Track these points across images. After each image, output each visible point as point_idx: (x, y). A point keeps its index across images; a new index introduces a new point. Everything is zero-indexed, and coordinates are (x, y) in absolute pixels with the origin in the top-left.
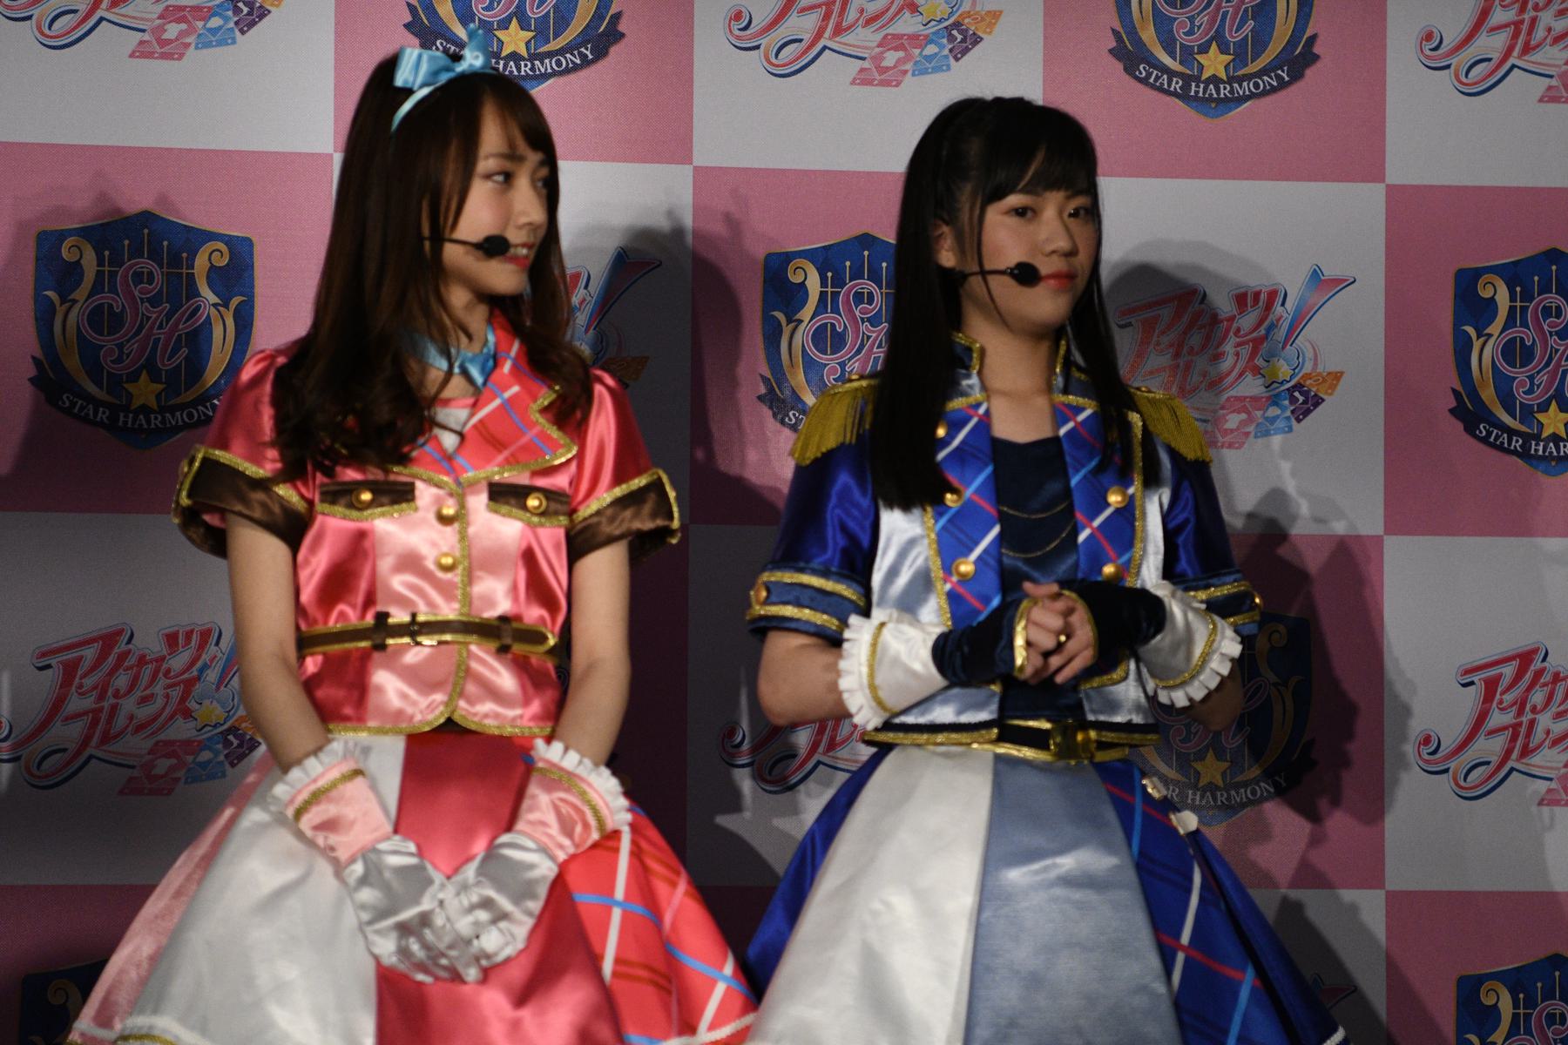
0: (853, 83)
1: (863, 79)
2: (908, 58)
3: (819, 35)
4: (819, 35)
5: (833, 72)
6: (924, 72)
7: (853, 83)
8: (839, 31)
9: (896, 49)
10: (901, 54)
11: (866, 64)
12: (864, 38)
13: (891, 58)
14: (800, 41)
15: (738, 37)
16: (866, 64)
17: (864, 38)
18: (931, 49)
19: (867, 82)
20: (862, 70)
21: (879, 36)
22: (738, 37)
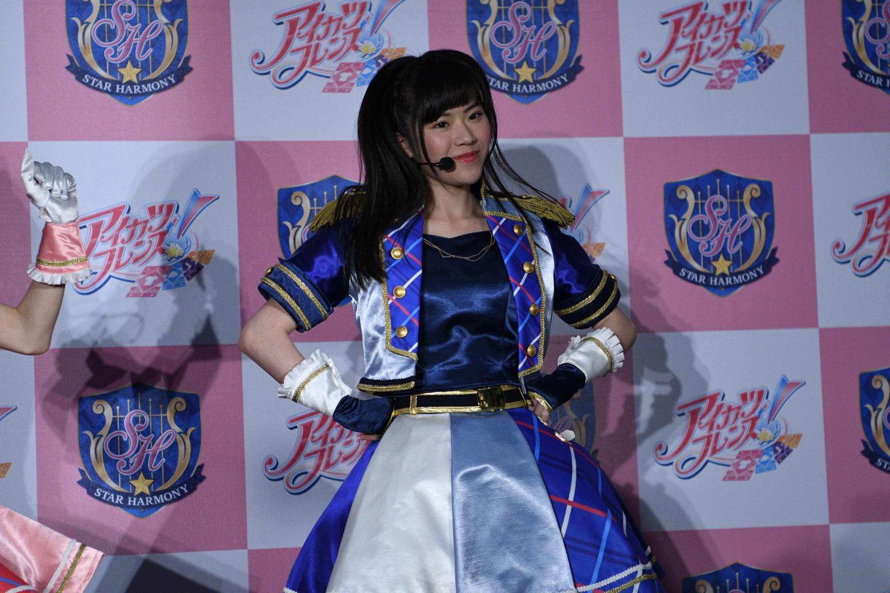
0: (324, 91)
1: (329, 89)
2: (354, 76)
3: (303, 65)
4: (303, 65)
5: (312, 85)
7: (324, 91)
8: (314, 62)
9: (347, 71)
10: (350, 74)
11: (331, 81)
13: (344, 76)
14: (293, 68)
15: (258, 68)
16: (331, 81)
19: (332, 91)
20: (329, 84)
21: (337, 64)
22: (258, 68)
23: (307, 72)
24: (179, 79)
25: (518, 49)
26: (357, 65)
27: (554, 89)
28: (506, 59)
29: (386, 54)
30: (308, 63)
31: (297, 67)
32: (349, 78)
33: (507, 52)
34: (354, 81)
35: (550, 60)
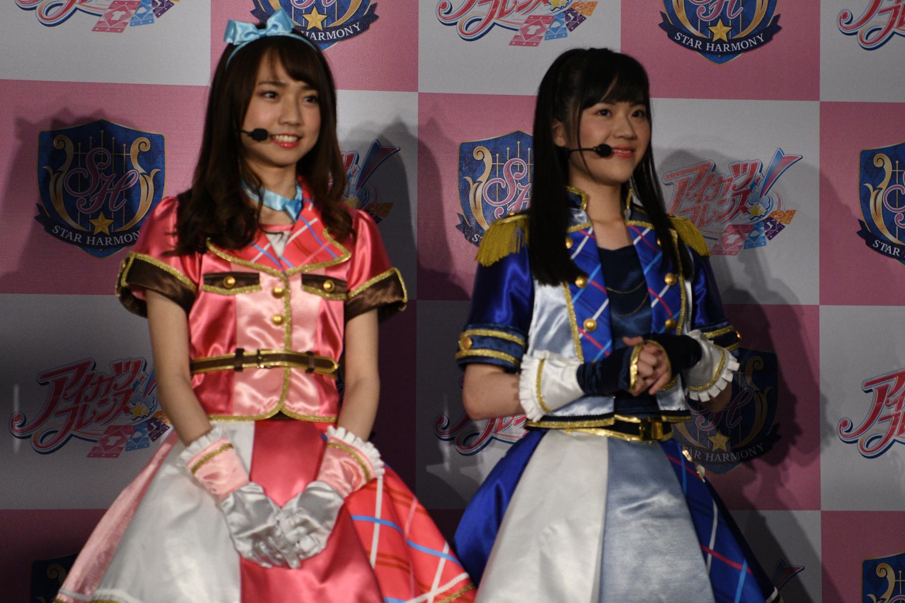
0: (511, 44)
1: (517, 42)
2: (543, 29)
3: (491, 16)
4: (491, 16)
5: (499, 37)
6: (552, 37)
7: (511, 44)
8: (502, 14)
9: (536, 24)
10: (538, 27)
11: (518, 33)
12: (517, 18)
13: (533, 30)
14: (480, 20)
15: (444, 18)
16: (518, 33)
17: (517, 18)
18: (556, 24)
19: (519, 44)
20: (516, 37)
21: (526, 17)
22: (444, 18)
23: (494, 24)
24: (365, 27)
25: (714, 6)
26: (546, 18)
27: (749, 49)
28: (701, 17)
29: (577, 8)
30: (496, 15)
31: (484, 18)
32: (538, 31)
33: (702, 9)
34: (543, 34)
35: (747, 19)
